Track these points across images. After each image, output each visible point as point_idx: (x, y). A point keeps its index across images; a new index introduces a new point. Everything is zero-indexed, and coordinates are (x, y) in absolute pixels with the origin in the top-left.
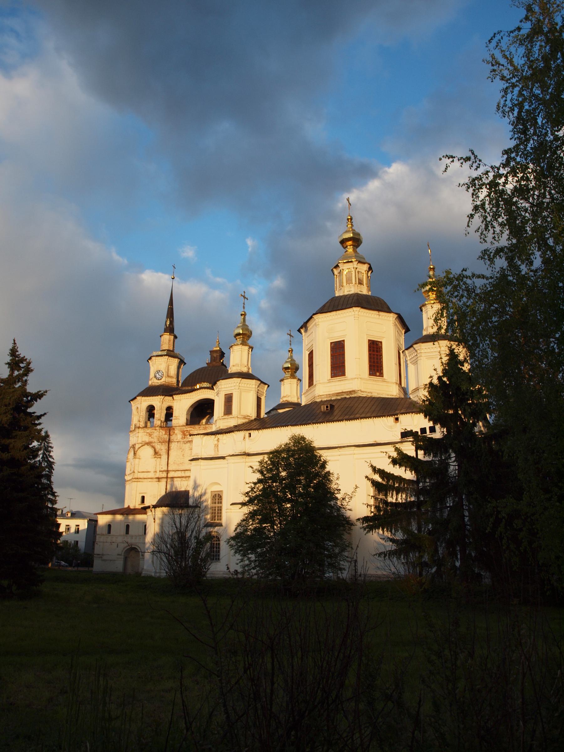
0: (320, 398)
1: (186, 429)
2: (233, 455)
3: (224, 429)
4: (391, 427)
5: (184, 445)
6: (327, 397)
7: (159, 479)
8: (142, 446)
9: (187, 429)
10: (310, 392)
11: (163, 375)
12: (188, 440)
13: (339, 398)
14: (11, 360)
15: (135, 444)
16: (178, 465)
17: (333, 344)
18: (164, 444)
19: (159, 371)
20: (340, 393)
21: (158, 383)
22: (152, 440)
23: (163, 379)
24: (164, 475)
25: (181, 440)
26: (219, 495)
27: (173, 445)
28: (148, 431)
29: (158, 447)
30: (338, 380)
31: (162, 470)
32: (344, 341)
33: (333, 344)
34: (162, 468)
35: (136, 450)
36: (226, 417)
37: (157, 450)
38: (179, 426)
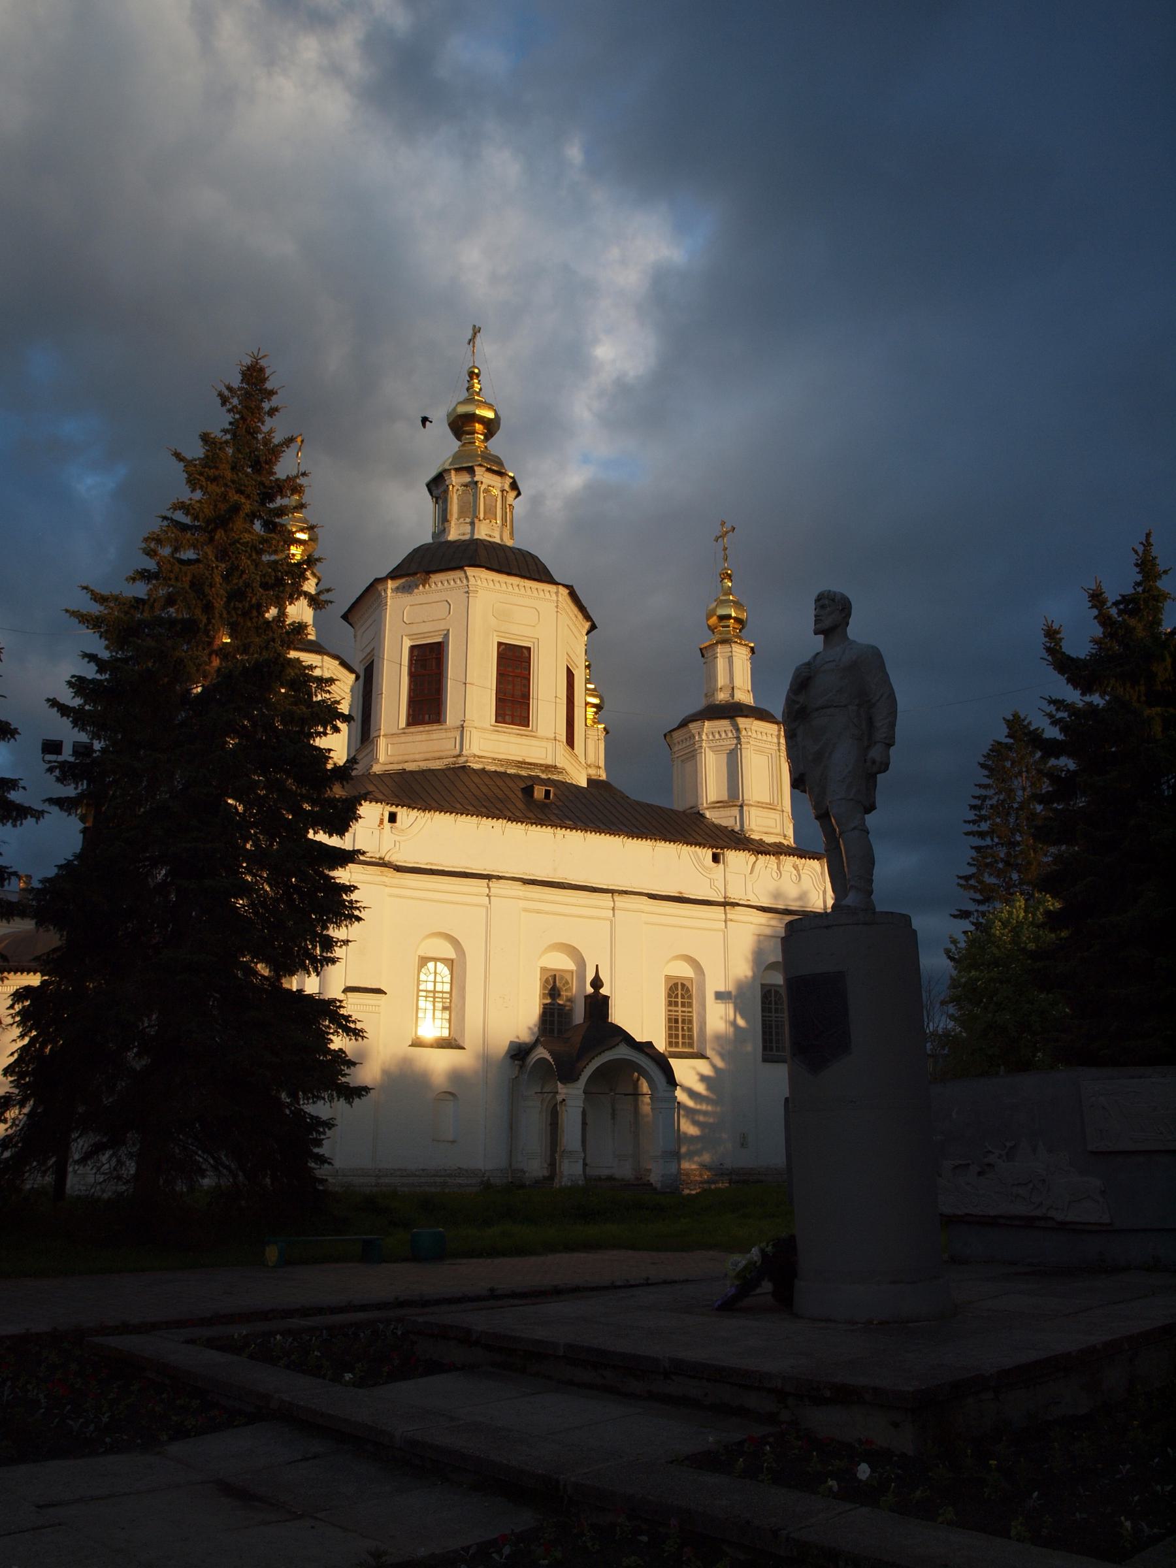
0: (482, 762)
6: (496, 765)
13: (523, 773)
33: (503, 647)
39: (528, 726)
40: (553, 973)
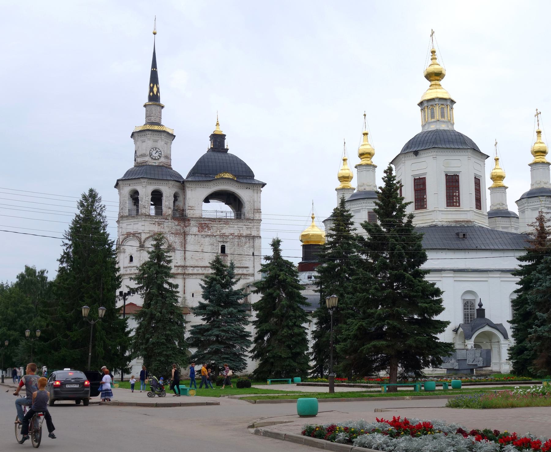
1: (203, 222)
5: (202, 239)
9: (205, 222)
11: (161, 154)
16: (197, 260)
18: (177, 236)
19: (156, 148)
20: (458, 221)
21: (155, 163)
25: (198, 233)
27: (189, 238)
31: (177, 265)
34: (177, 263)
37: (170, 242)
38: (195, 218)
40: (467, 301)
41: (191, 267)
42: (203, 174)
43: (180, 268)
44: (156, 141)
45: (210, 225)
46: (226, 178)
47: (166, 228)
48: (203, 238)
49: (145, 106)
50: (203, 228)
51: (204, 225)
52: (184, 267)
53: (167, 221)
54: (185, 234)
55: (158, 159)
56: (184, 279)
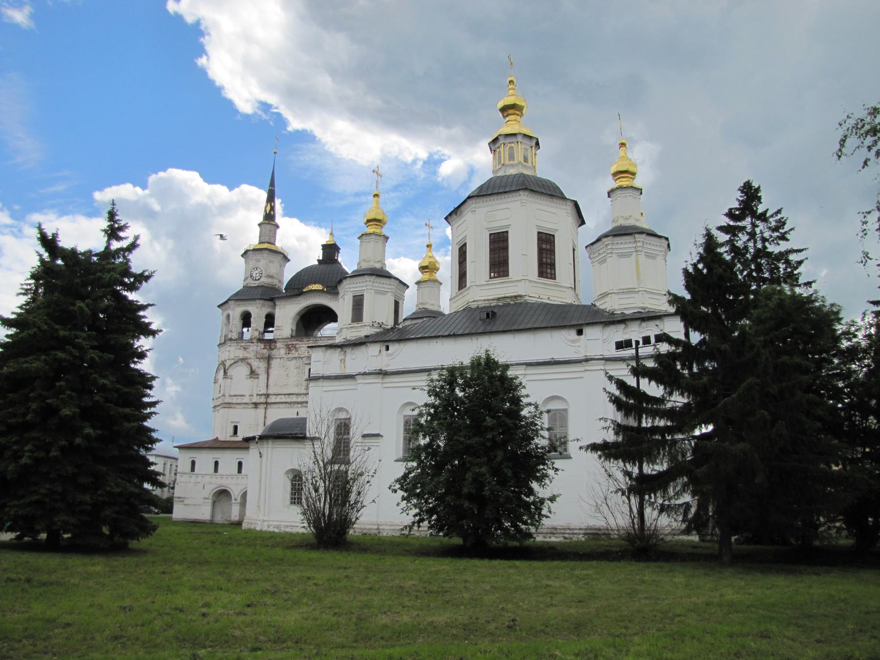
1: (291, 343)
2: (365, 374)
3: (353, 341)
4: (573, 341)
7: (256, 405)
8: (235, 363)
9: (293, 343)
10: (461, 296)
12: (293, 356)
14: (108, 226)
15: (226, 361)
16: (280, 387)
17: (492, 236)
18: (262, 360)
22: (247, 355)
23: (262, 280)
24: (263, 400)
25: (284, 356)
26: (345, 424)
27: (274, 363)
28: (242, 344)
29: (256, 364)
30: (499, 281)
31: (260, 393)
32: (507, 232)
35: (227, 368)
36: (355, 325)
37: (254, 368)
38: (283, 339)
39: (508, 275)
41: (275, 395)
42: (296, 289)
43: (263, 397)
44: (258, 261)
45: (297, 346)
46: (315, 290)
47: (251, 352)
48: (289, 361)
49: (260, 225)
50: (290, 350)
51: (291, 346)
52: (267, 396)
53: (252, 344)
54: (269, 359)
55: (259, 279)
56: (266, 408)
